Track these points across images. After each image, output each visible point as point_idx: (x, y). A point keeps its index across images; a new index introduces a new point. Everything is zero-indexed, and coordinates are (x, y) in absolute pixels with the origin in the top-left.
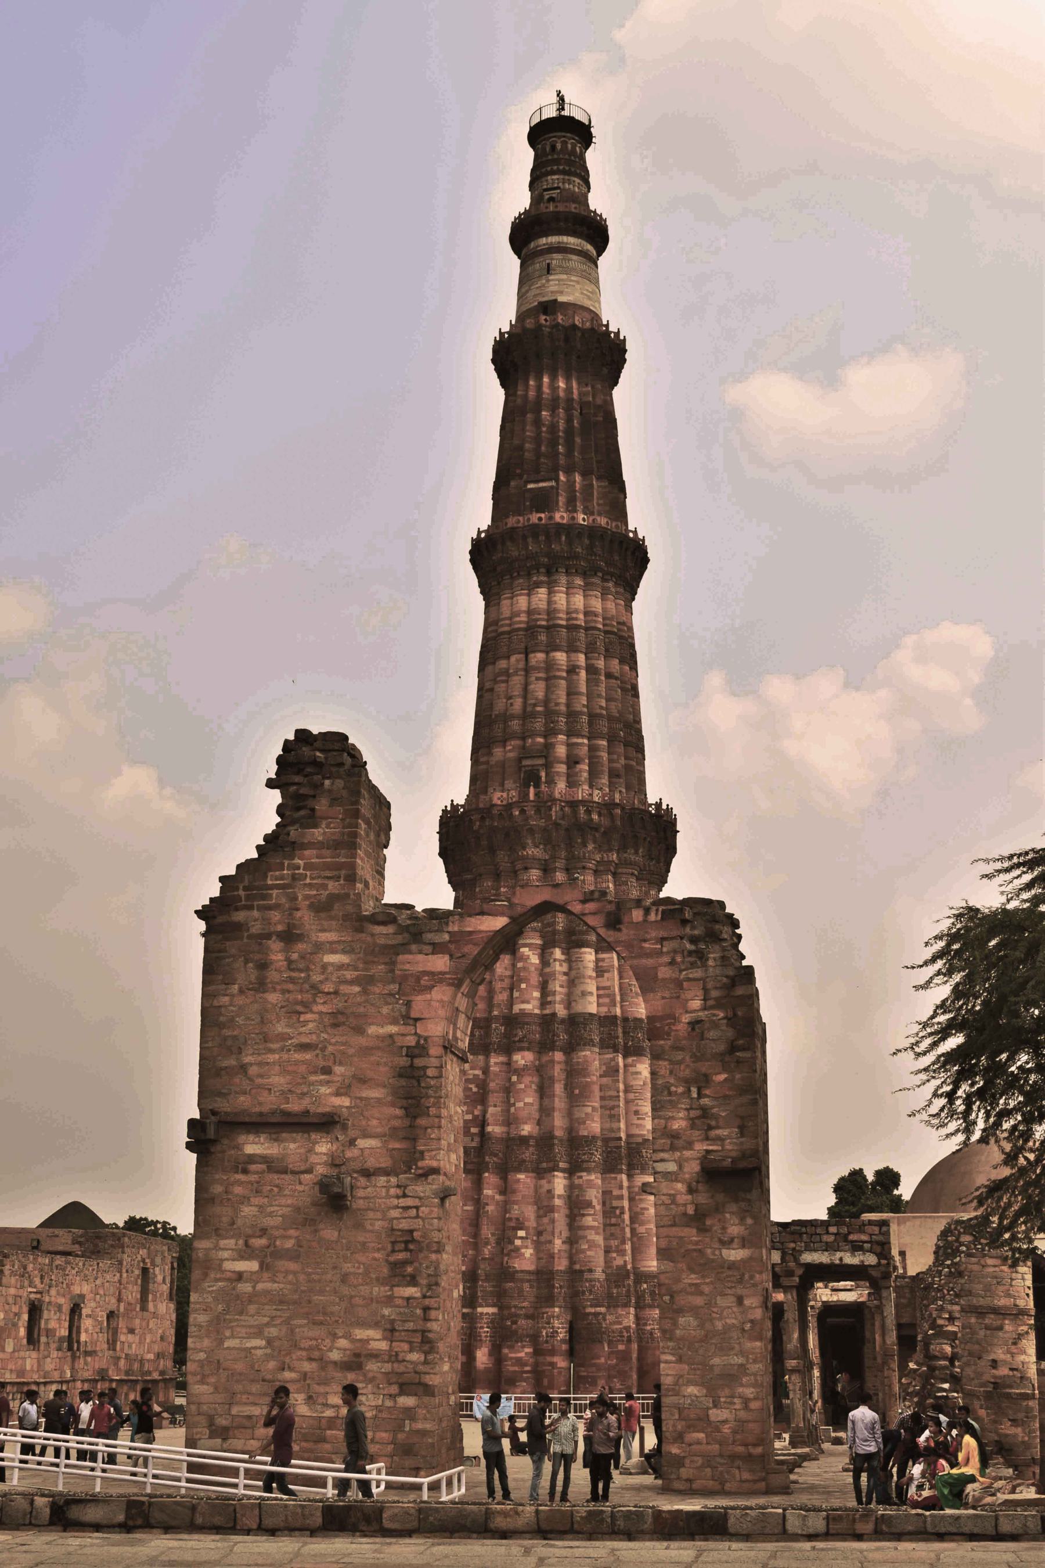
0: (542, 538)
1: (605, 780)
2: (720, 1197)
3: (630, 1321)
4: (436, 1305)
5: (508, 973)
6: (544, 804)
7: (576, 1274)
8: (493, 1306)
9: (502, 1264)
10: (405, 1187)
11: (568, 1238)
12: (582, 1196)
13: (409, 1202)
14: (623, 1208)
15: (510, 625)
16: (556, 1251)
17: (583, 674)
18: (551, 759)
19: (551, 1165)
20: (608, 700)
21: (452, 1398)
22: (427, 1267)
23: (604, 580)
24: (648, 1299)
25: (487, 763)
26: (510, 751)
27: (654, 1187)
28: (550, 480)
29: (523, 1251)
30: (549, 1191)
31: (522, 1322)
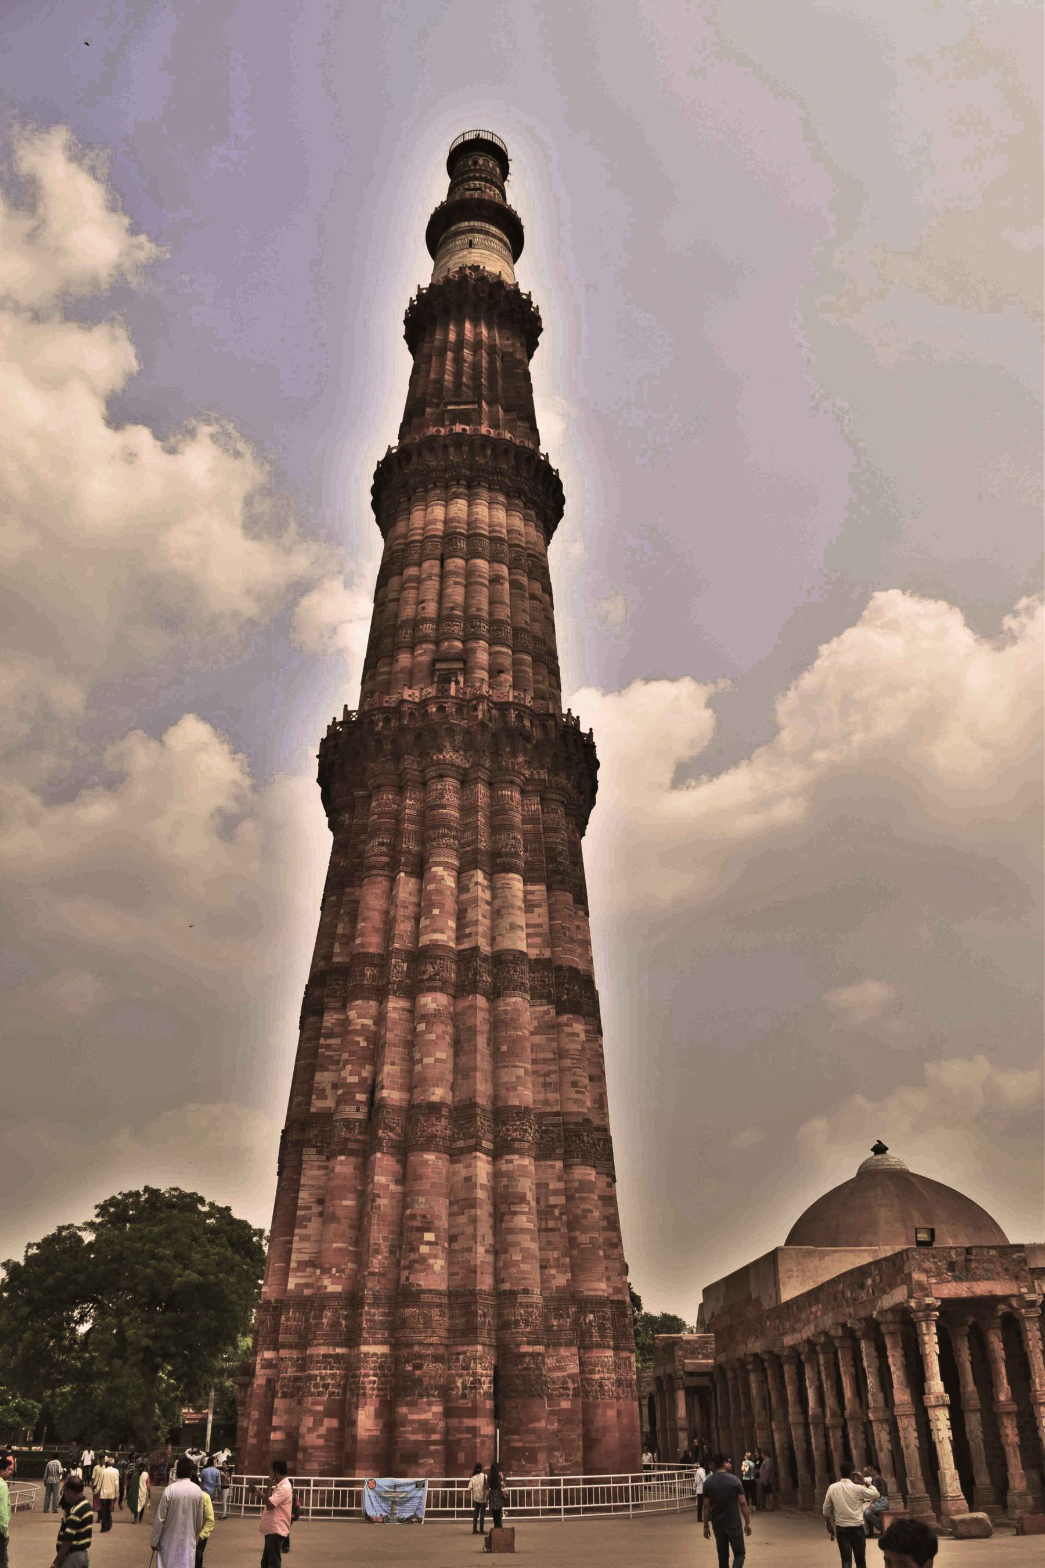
0: (465, 449)
5: (414, 899)
7: (505, 1298)
8: (382, 1343)
9: (399, 1279)
11: (493, 1246)
12: (513, 1187)
15: (423, 535)
16: (479, 1263)
17: (507, 585)
18: (469, 665)
19: (472, 1142)
24: (596, 1338)
26: (421, 655)
29: (431, 1261)
30: (468, 1179)
31: (429, 1367)
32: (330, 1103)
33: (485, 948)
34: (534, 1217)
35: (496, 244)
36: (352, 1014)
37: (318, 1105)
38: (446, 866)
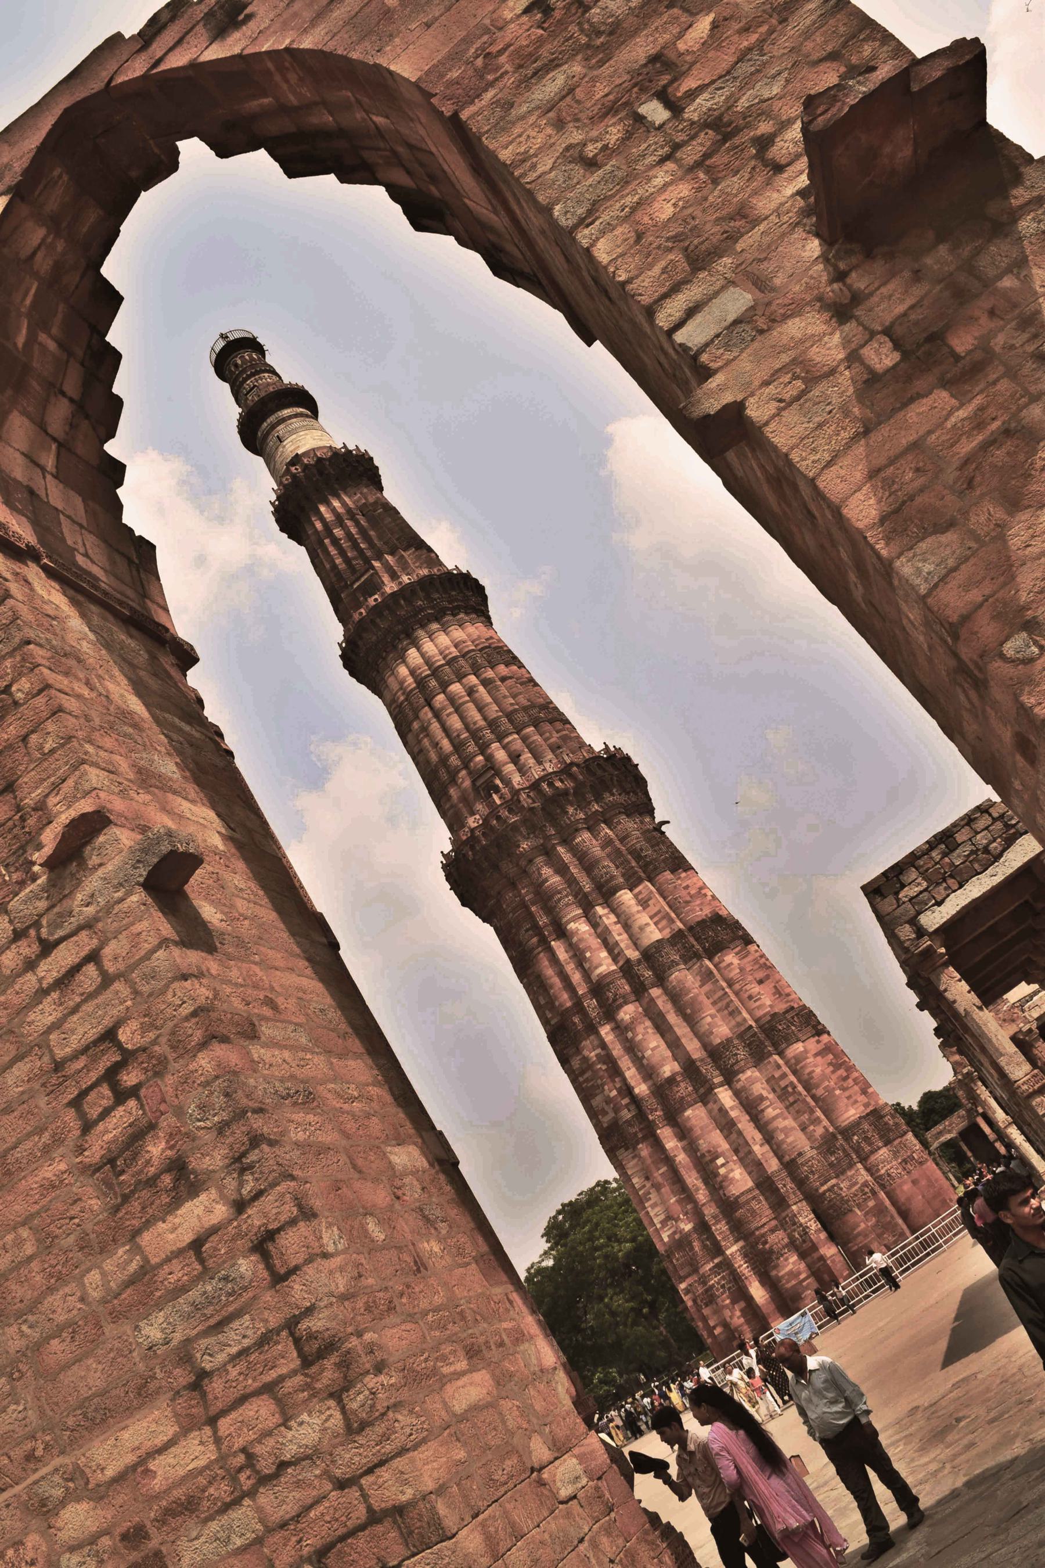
0: (386, 613)
1: (550, 756)
2: (941, 258)
3: (864, 1176)
4: (290, 1210)
6: (513, 803)
7: (790, 1166)
8: (736, 1241)
10: (37, 924)
13: (64, 957)
14: (792, 1083)
17: (481, 689)
19: (707, 1086)
20: (514, 697)
21: (567, 1474)
22: (202, 1107)
23: (454, 615)
24: (867, 1149)
25: (452, 806)
27: (722, 389)
28: (367, 571)
31: (772, 1239)
32: (611, 1115)
33: (633, 954)
34: (779, 1104)
35: (296, 423)
36: (586, 1053)
37: (606, 1120)
38: (574, 919)
